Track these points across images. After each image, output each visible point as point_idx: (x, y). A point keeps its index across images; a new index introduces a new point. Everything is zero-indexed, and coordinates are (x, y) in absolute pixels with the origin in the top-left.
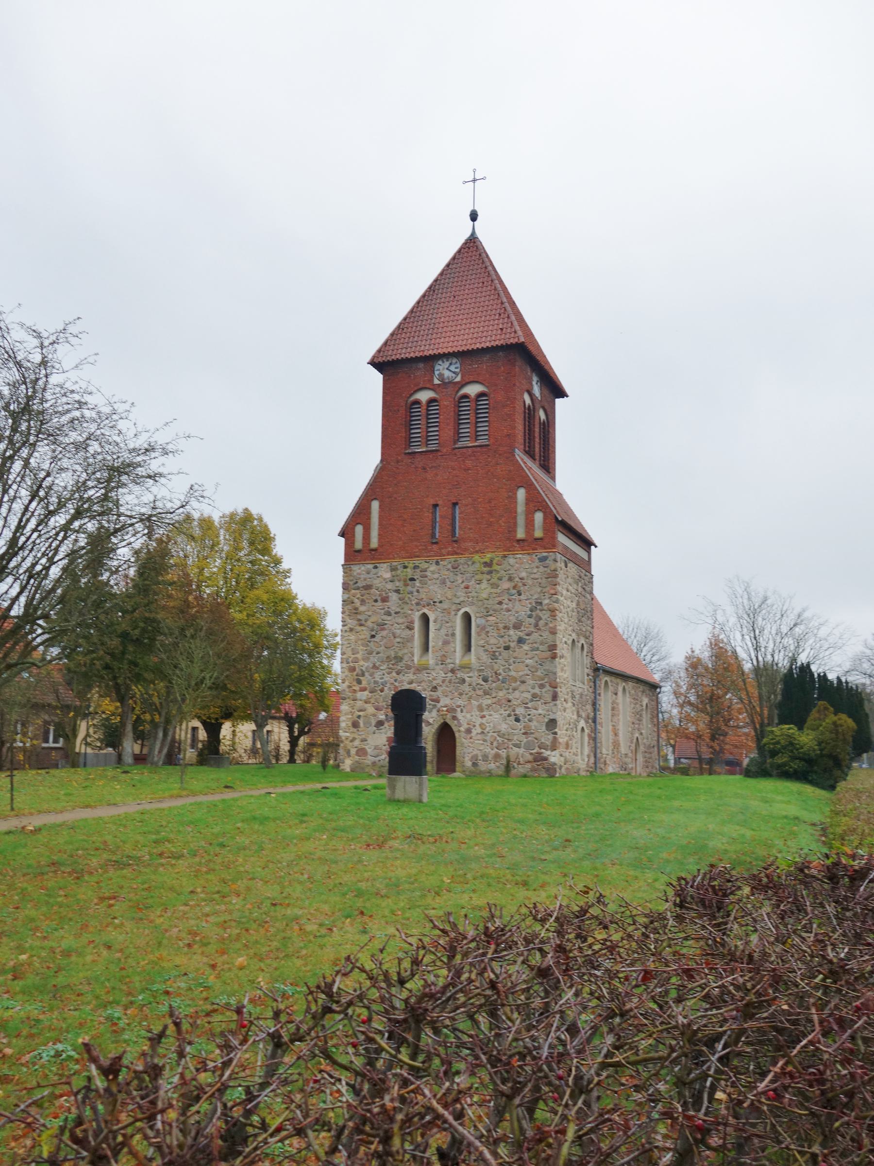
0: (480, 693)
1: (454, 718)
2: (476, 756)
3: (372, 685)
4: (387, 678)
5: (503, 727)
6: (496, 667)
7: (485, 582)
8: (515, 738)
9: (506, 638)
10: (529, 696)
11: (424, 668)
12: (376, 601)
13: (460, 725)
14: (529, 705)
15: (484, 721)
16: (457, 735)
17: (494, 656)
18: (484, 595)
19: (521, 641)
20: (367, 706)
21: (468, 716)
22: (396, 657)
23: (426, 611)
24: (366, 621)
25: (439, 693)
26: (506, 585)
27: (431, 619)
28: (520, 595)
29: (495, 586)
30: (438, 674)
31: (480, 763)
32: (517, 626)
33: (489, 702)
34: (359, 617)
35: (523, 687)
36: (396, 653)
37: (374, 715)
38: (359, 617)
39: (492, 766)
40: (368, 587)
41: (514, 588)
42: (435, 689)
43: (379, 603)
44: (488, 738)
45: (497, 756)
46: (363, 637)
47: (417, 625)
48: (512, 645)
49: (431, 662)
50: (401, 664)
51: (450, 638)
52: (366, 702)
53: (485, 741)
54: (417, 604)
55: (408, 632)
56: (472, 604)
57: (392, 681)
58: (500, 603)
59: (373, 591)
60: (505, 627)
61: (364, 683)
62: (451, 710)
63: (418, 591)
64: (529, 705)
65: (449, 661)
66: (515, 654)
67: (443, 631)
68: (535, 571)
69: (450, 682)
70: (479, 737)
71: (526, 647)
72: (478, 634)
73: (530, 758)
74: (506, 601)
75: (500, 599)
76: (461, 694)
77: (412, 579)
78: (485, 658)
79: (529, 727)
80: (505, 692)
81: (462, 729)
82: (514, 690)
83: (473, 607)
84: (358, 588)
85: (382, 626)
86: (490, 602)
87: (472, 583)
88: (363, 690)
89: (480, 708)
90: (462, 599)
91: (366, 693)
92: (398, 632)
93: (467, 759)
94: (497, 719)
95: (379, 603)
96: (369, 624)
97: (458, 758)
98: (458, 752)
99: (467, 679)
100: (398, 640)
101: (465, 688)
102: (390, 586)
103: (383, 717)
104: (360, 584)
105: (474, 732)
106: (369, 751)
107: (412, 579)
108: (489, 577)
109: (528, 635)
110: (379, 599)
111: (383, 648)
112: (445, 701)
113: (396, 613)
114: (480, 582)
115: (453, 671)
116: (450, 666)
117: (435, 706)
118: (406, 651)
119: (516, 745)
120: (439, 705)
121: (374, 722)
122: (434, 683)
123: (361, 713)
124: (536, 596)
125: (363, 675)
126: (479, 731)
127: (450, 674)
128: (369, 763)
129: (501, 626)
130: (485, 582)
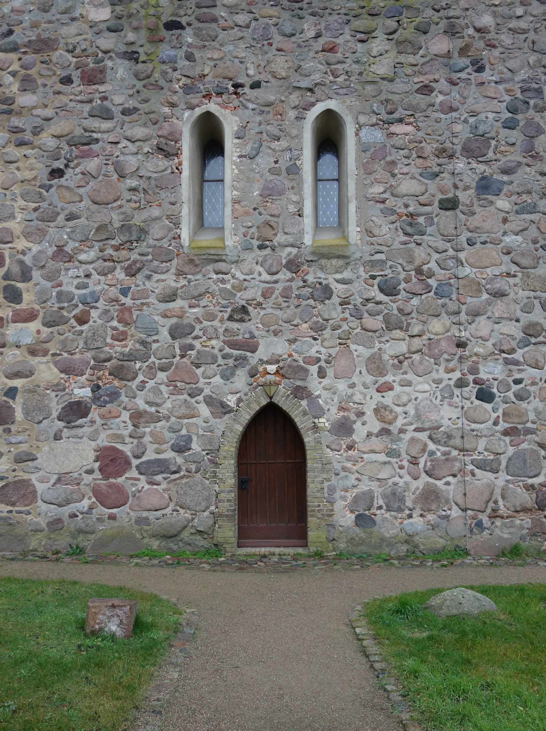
0: (376, 323)
1: (300, 392)
2: (369, 496)
3: (53, 305)
4: (97, 284)
5: (447, 416)
6: (420, 254)
7: (380, 34)
8: (482, 445)
9: (447, 180)
10: (514, 330)
11: (215, 258)
12: (67, 81)
13: (319, 412)
14: (518, 355)
15: (388, 398)
16: (308, 439)
17: (411, 225)
18: (382, 68)
19: (485, 186)
20: (35, 361)
21: (342, 386)
22: (125, 228)
23: (213, 107)
24: (37, 131)
25: (254, 325)
26: (440, 44)
27: (230, 125)
28: (480, 69)
29: (403, 46)
30: (251, 275)
31: (381, 515)
32: (474, 150)
33: (402, 348)
34: (16, 121)
35: (499, 308)
36: (127, 218)
37: (58, 388)
38: (16, 121)
39: (417, 523)
40: (43, 45)
41: (464, 51)
42: (241, 313)
43: (77, 87)
44: (402, 447)
45: (430, 498)
46: (28, 175)
47: (187, 146)
48: (464, 197)
49: (231, 241)
50: (143, 247)
51: (284, 181)
52: (33, 352)
53: (391, 453)
54: (188, 90)
55: (162, 163)
56: (347, 90)
57: (114, 292)
58: (426, 89)
59: (59, 55)
60: (441, 152)
61: (29, 299)
62: (290, 370)
63: (190, 57)
64: (518, 355)
65: (280, 238)
66: (474, 221)
67: (265, 161)
68: (520, 11)
69: (286, 294)
70: (377, 443)
71: (503, 203)
72: (366, 169)
73: (527, 499)
74: (443, 85)
75: (424, 79)
76: (318, 328)
77: (173, 26)
78: (385, 229)
79: (522, 414)
80: (446, 320)
81: (323, 422)
82: (475, 314)
83: (351, 100)
84: (14, 49)
85: (85, 143)
86: (399, 86)
87: (345, 38)
88: (30, 316)
89: (376, 365)
90: (317, 77)
91: (34, 326)
92: (131, 162)
93: (340, 504)
94: (425, 396)
95: (77, 87)
96: (46, 139)
97: (312, 502)
98: (312, 487)
99: (334, 286)
100: (132, 183)
101: (332, 310)
102: (107, 42)
103: (83, 393)
104: (18, 37)
105: (360, 431)
106: (40, 487)
107: (173, 26)
108: (392, 24)
109: (505, 172)
110: (76, 75)
111: (86, 202)
112: (271, 347)
113: (126, 112)
114: (366, 36)
115: (293, 266)
116: (286, 253)
117: (241, 361)
118: (156, 212)
119: (482, 465)
120: (254, 359)
121: (56, 409)
122: (241, 298)
123: (18, 383)
124: (523, 75)
125: (26, 276)
126: (376, 426)
127: (284, 275)
128: (42, 522)
129: (429, 148)
130: (380, 34)
